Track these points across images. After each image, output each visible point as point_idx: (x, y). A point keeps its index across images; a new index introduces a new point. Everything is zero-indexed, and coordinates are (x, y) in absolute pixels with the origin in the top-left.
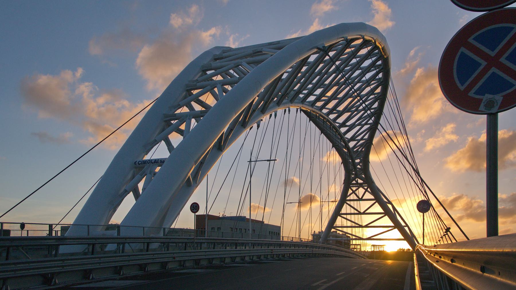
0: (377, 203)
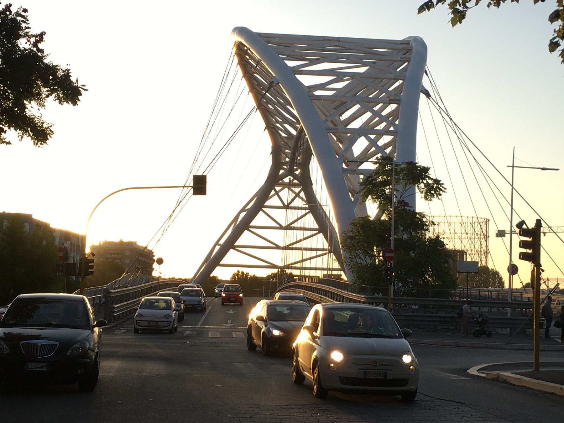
0: (310, 214)
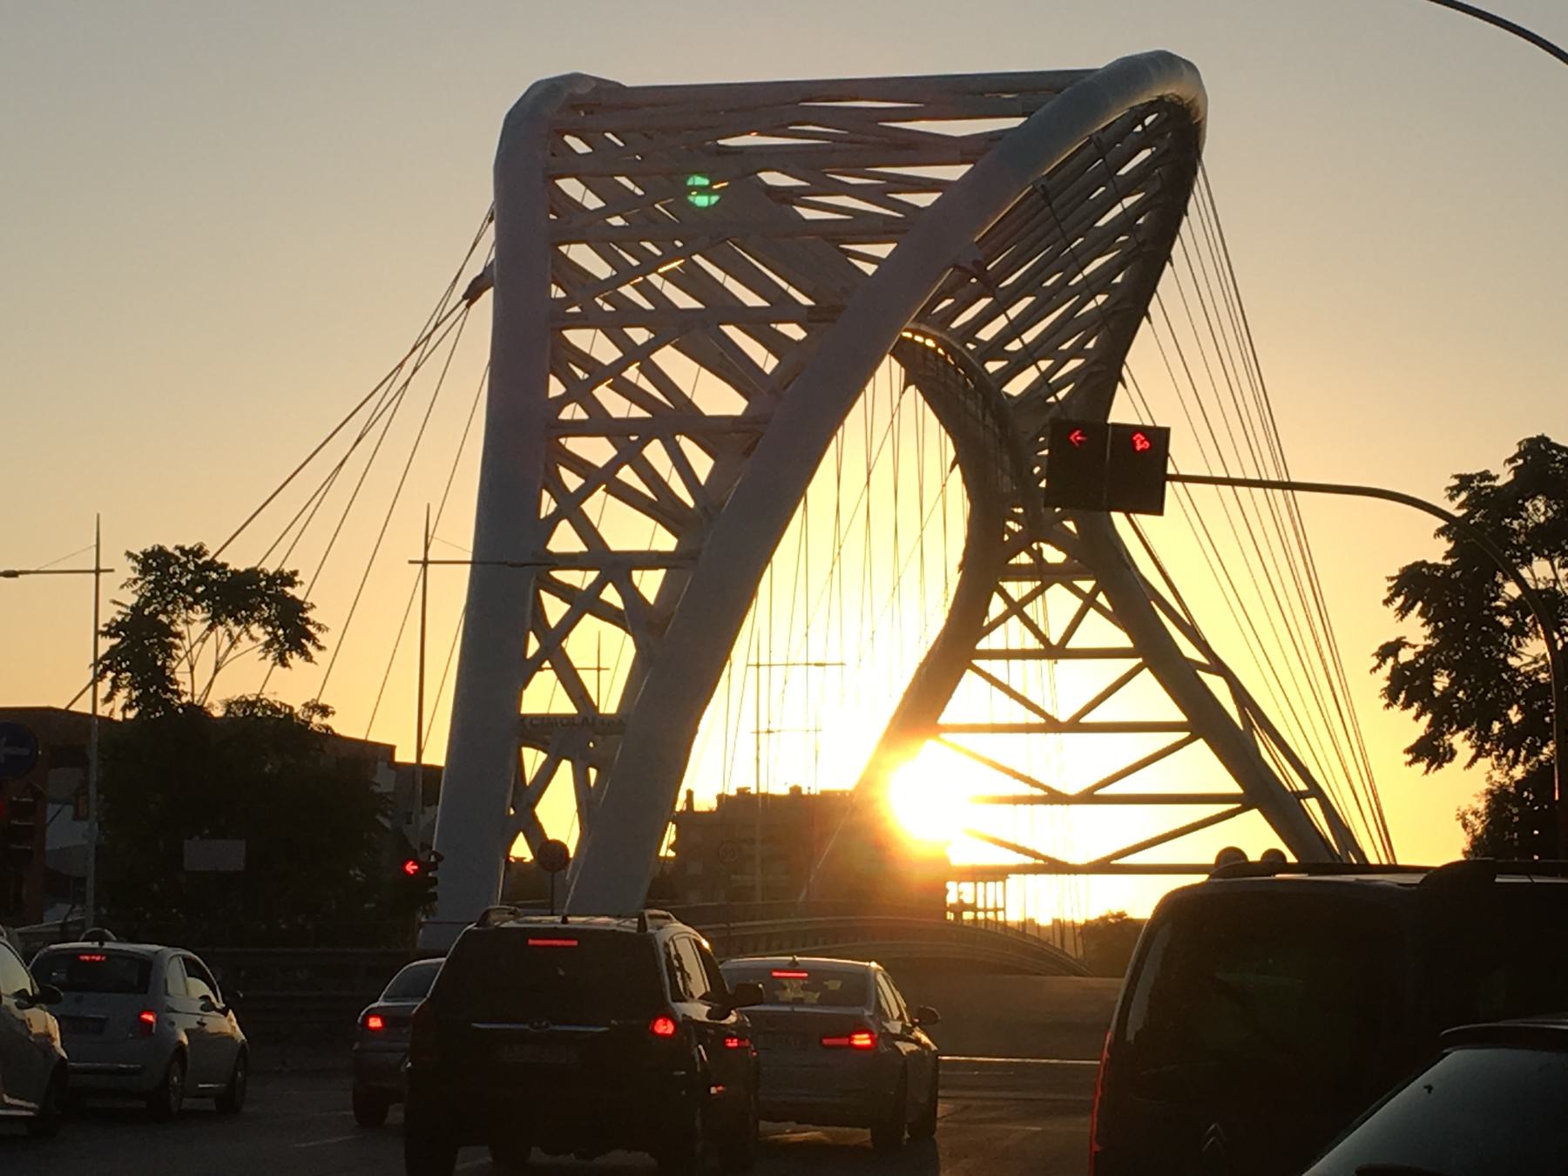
0: (1146, 671)
